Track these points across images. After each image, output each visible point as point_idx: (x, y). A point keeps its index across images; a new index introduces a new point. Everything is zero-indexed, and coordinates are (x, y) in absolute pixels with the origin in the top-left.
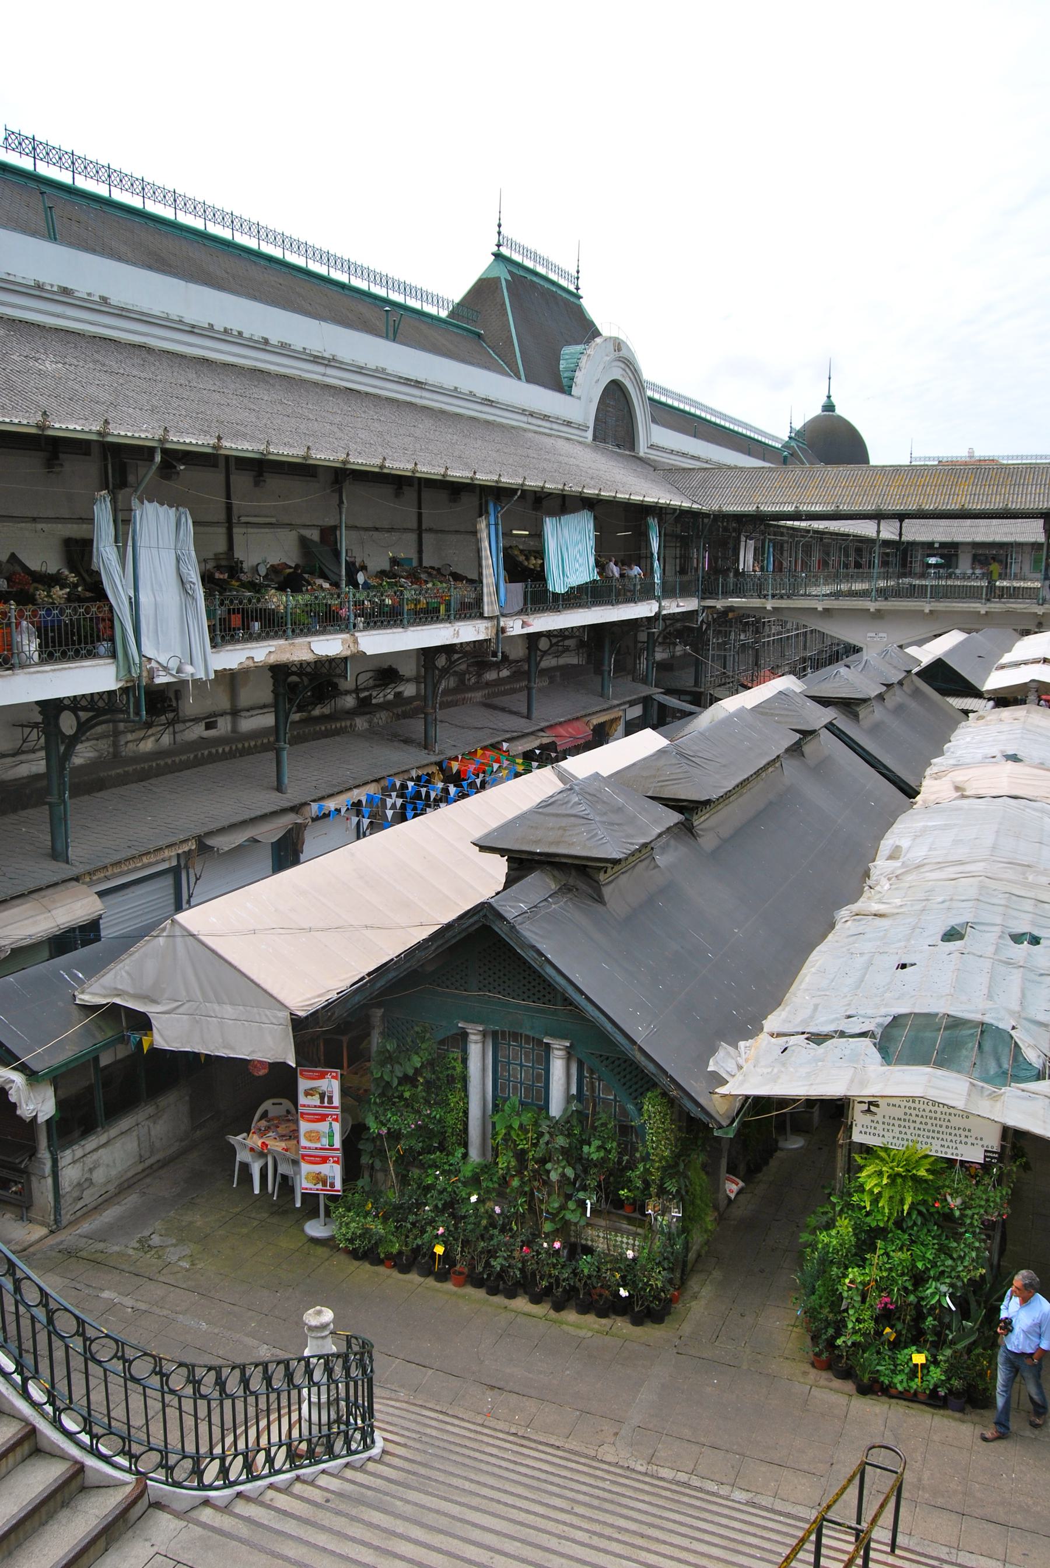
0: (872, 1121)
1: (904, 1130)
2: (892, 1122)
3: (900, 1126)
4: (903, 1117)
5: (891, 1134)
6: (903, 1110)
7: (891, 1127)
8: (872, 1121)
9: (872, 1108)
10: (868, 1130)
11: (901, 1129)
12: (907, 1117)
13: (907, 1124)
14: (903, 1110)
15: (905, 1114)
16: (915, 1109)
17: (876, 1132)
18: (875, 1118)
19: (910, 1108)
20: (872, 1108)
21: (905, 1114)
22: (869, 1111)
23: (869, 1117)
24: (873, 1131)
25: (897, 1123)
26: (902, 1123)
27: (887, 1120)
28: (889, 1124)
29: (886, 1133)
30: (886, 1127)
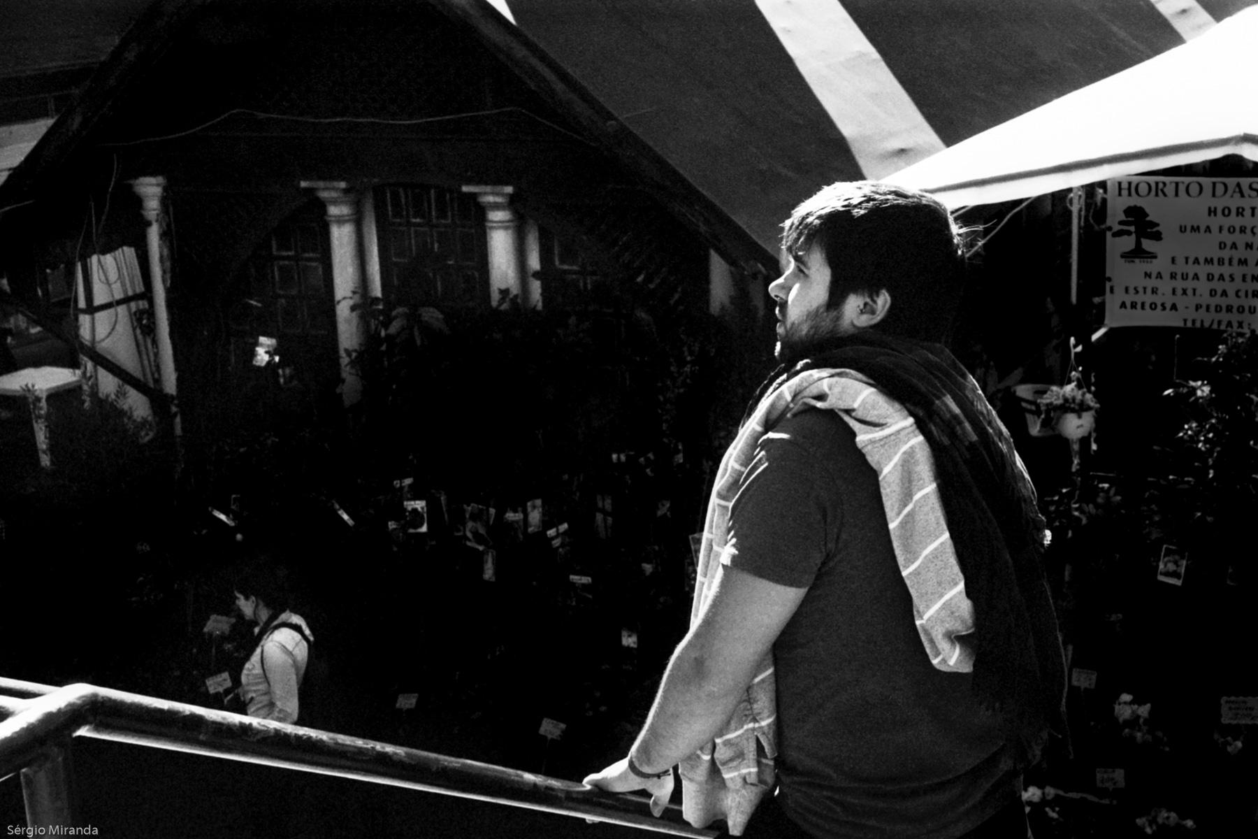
0: (1148, 275)
1: (1219, 286)
2: (1191, 269)
3: (1210, 277)
4: (1216, 254)
5: (1191, 301)
6: (1216, 237)
7: (1190, 284)
8: (1148, 275)
9: (1147, 244)
10: (1139, 299)
11: (1216, 284)
12: (1226, 254)
13: (1226, 270)
14: (1216, 237)
15: (1222, 246)
16: (1243, 230)
17: (1158, 300)
18: (1153, 266)
19: (1231, 230)
20: (1147, 244)
21: (1222, 246)
22: (1138, 253)
23: (1140, 266)
24: (1149, 298)
25: (1203, 270)
26: (1216, 270)
27: (1180, 268)
28: (1185, 277)
29: (1180, 301)
30: (1179, 284)
